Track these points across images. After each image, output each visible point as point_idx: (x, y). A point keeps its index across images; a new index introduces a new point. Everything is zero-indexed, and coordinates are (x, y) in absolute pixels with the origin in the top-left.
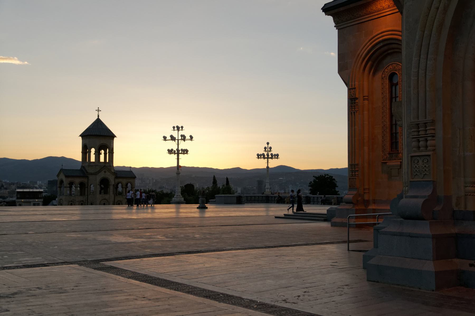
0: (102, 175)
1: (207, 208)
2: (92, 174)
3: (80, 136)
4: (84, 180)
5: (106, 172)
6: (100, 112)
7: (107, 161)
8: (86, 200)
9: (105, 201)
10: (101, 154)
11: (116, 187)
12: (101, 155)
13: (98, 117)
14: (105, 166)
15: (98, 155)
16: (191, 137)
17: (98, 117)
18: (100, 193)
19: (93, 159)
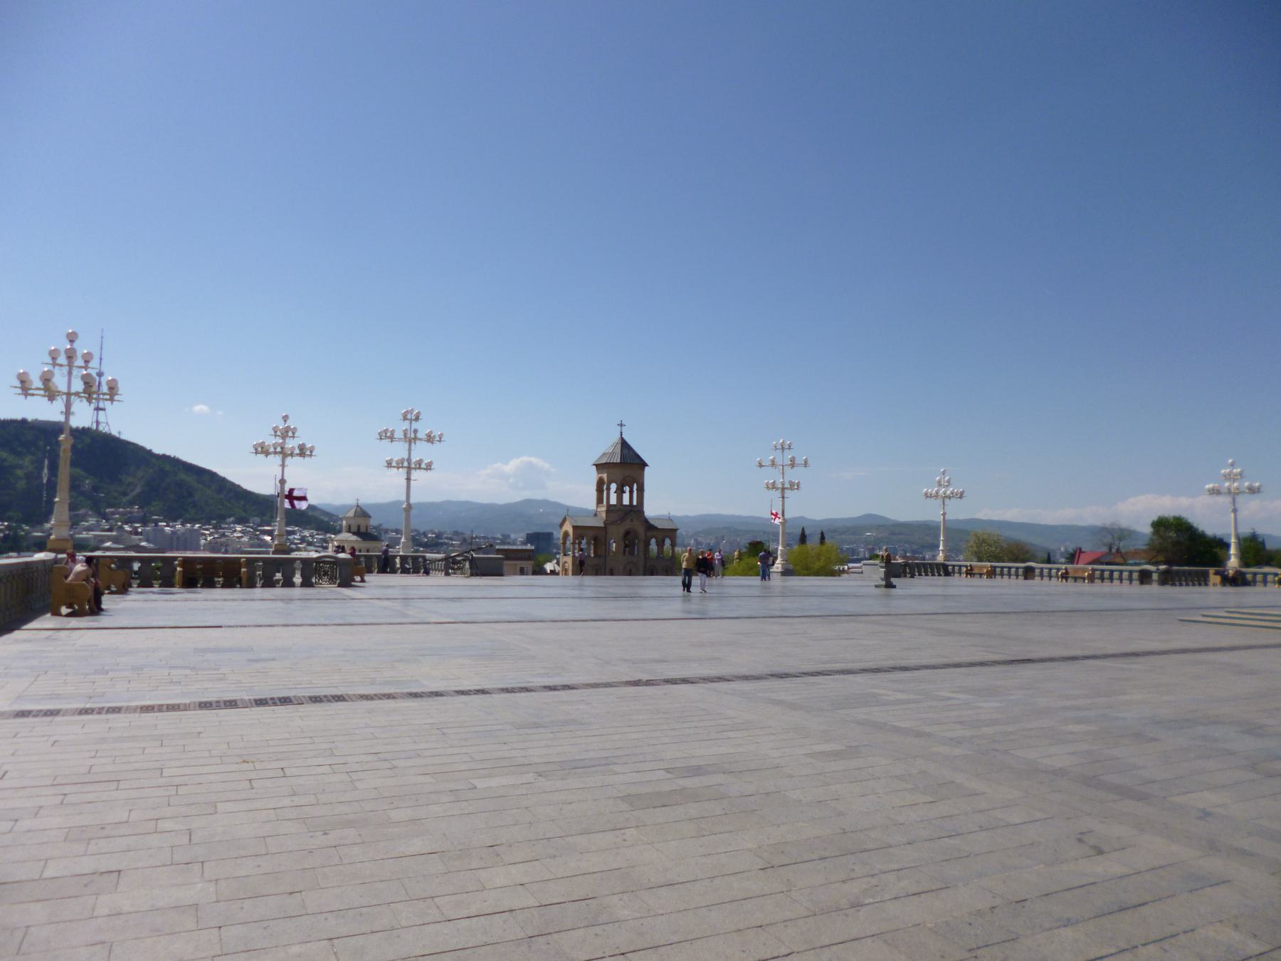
0: (627, 525)
1: (894, 587)
7: (635, 503)
10: (625, 492)
11: (647, 544)
12: (624, 494)
13: (621, 435)
15: (620, 492)
16: (806, 464)
17: (621, 435)
18: (624, 554)
19: (613, 501)
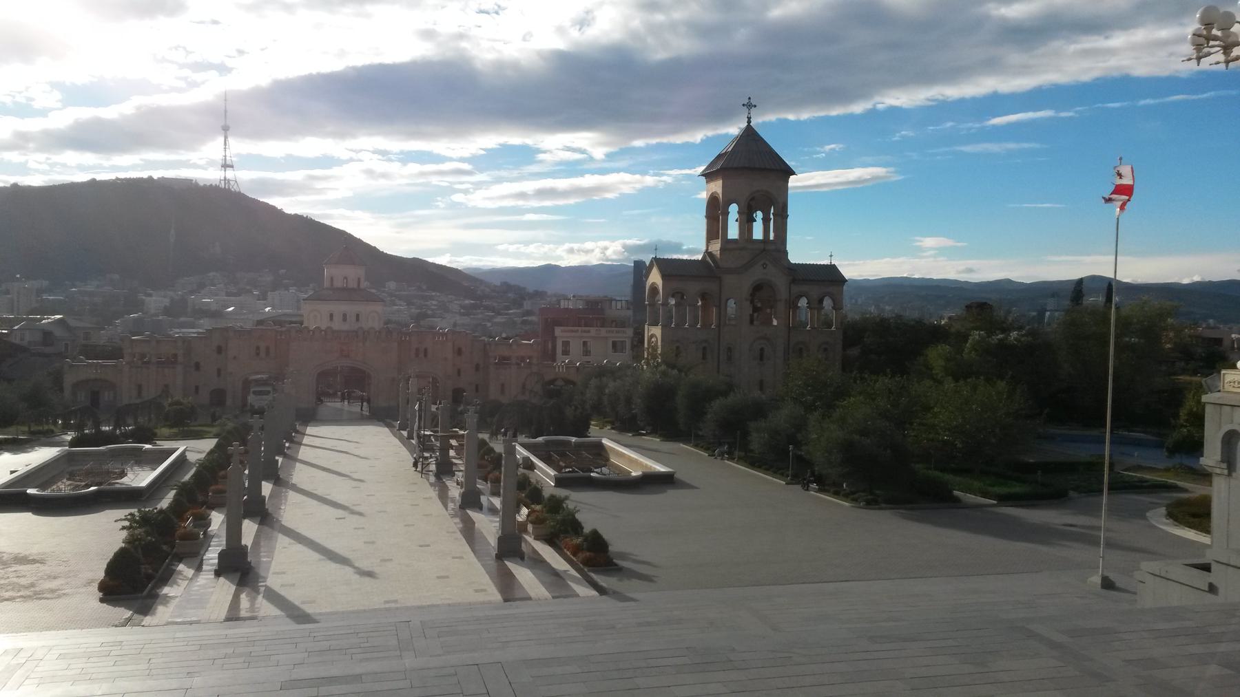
0: (757, 274)
5: (766, 265)
7: (772, 237)
11: (793, 305)
12: (754, 223)
14: (764, 250)
15: (746, 221)
18: (752, 322)
19: (733, 232)
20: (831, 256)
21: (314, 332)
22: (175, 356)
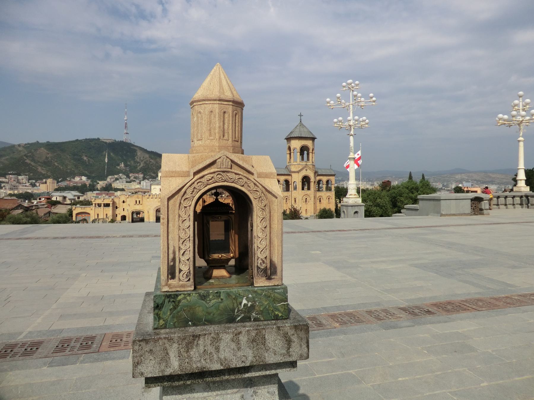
0: (304, 173)
2: (294, 172)
3: (285, 139)
4: (288, 178)
6: (302, 117)
8: (290, 196)
9: (306, 196)
18: (303, 189)
20: (331, 166)
21: (155, 195)
22: (109, 204)
